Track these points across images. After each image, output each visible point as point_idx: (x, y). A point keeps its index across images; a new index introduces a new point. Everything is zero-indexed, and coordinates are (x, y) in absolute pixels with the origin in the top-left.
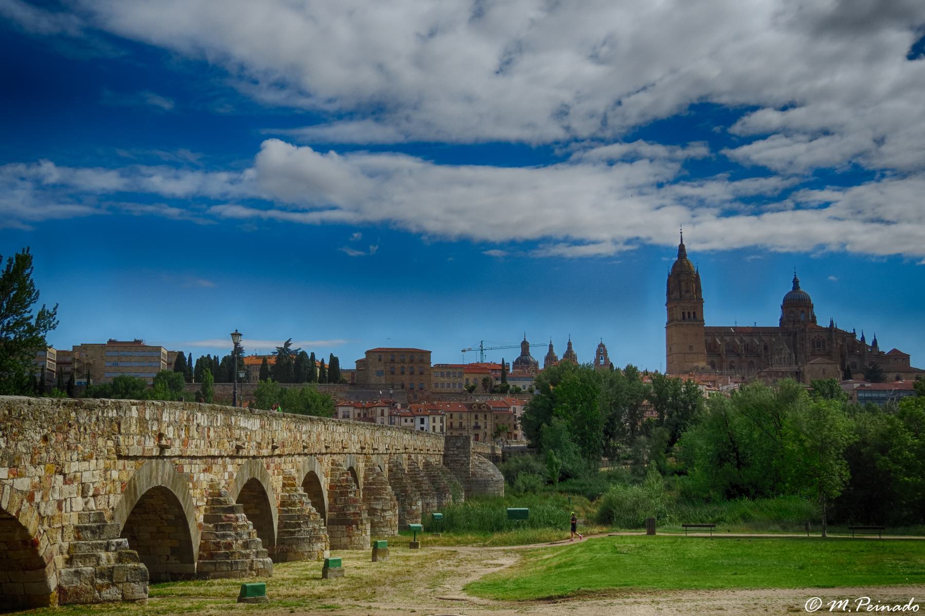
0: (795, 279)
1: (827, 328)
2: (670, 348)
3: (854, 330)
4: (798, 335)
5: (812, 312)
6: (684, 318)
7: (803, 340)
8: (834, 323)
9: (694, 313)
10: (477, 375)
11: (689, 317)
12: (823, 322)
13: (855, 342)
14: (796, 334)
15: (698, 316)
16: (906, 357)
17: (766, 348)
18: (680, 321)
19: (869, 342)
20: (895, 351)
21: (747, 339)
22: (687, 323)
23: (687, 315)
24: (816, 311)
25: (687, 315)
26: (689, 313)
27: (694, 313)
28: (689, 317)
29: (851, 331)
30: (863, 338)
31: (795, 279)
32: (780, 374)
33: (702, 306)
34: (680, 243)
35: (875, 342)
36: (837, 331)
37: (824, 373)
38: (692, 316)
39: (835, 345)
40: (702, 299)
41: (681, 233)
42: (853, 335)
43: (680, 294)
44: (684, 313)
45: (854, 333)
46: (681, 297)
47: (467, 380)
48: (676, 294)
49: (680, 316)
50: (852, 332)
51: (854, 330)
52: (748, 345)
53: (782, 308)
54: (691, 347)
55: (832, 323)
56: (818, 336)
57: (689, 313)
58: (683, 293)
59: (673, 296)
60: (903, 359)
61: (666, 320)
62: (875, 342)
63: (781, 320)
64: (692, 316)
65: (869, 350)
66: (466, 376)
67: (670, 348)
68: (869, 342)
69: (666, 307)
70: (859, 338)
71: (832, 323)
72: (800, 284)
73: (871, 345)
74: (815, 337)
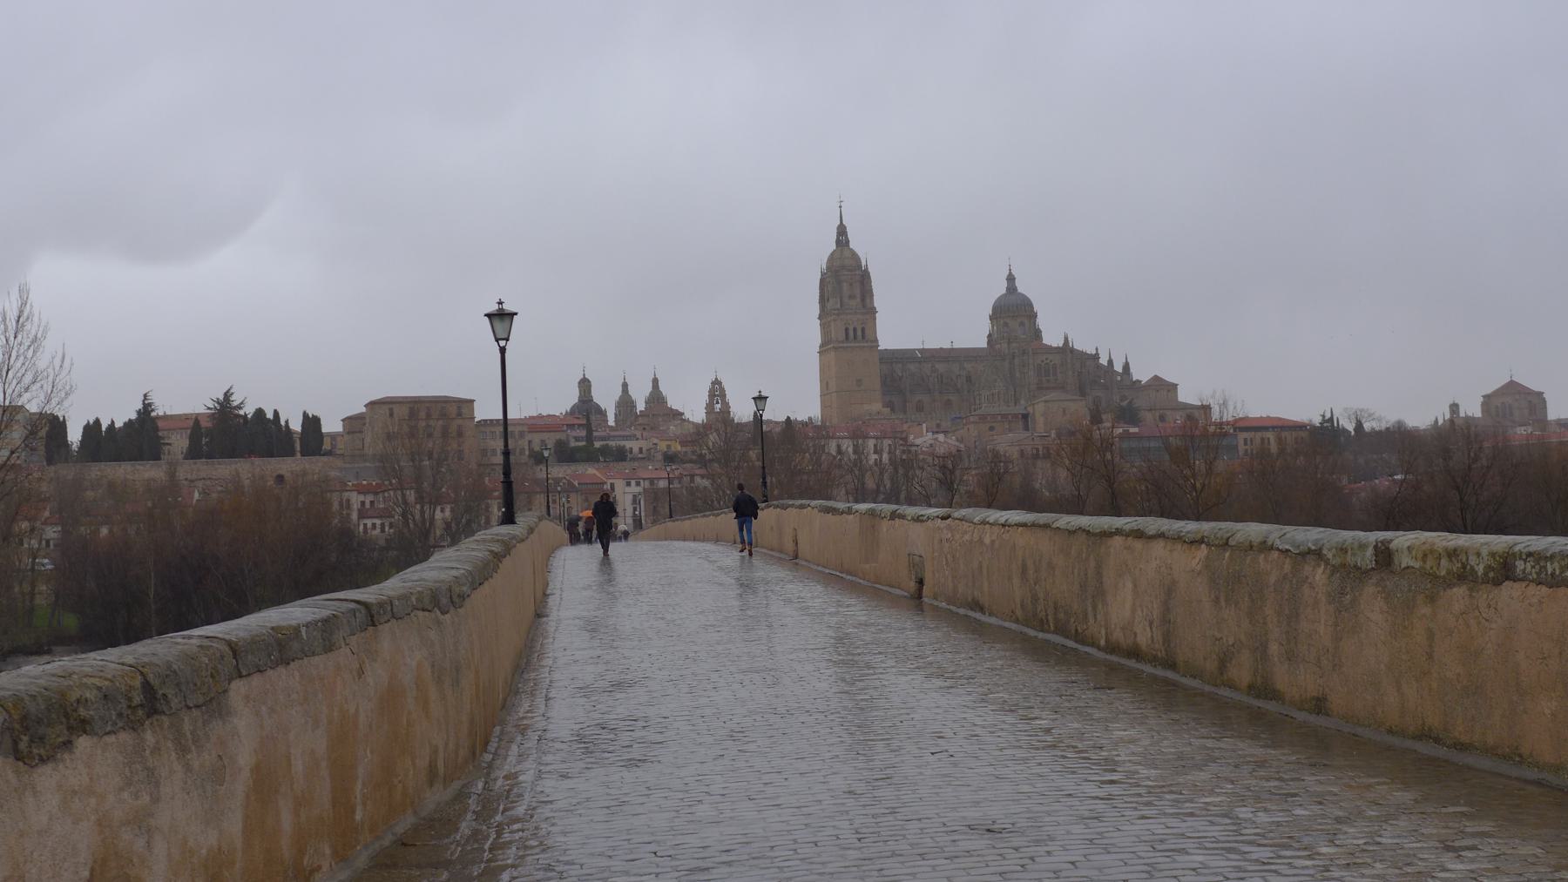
0: (1010, 274)
1: (1058, 348)
2: (827, 383)
3: (1097, 349)
4: (1016, 361)
5: (1035, 324)
7: (1024, 366)
8: (1069, 339)
10: (545, 434)
11: (855, 338)
12: (1052, 338)
13: (1099, 366)
14: (1014, 357)
15: (867, 332)
16: (1173, 387)
17: (969, 379)
18: (843, 342)
19: (1118, 368)
20: (1156, 378)
21: (941, 367)
22: (852, 345)
24: (1042, 322)
26: (855, 330)
28: (855, 338)
29: (1091, 351)
30: (1110, 362)
31: (1010, 274)
32: (999, 418)
33: (875, 319)
34: (839, 223)
35: (1126, 367)
36: (1072, 350)
38: (859, 333)
39: (1070, 373)
40: (875, 308)
41: (840, 207)
42: (1096, 357)
43: (841, 301)
44: (847, 330)
45: (1097, 354)
46: (841, 306)
47: (530, 442)
48: (833, 304)
49: (842, 336)
50: (1094, 352)
51: (1097, 349)
52: (942, 377)
53: (991, 319)
54: (859, 382)
55: (1066, 339)
56: (1047, 359)
57: (855, 330)
59: (829, 305)
60: (1169, 391)
61: (819, 341)
62: (1126, 367)
63: (990, 336)
64: (859, 333)
65: (1119, 378)
66: (529, 437)
67: (827, 383)
68: (1118, 368)
70: (1104, 361)
71: (1066, 339)
72: (1018, 283)
73: (1120, 371)
74: (1043, 361)
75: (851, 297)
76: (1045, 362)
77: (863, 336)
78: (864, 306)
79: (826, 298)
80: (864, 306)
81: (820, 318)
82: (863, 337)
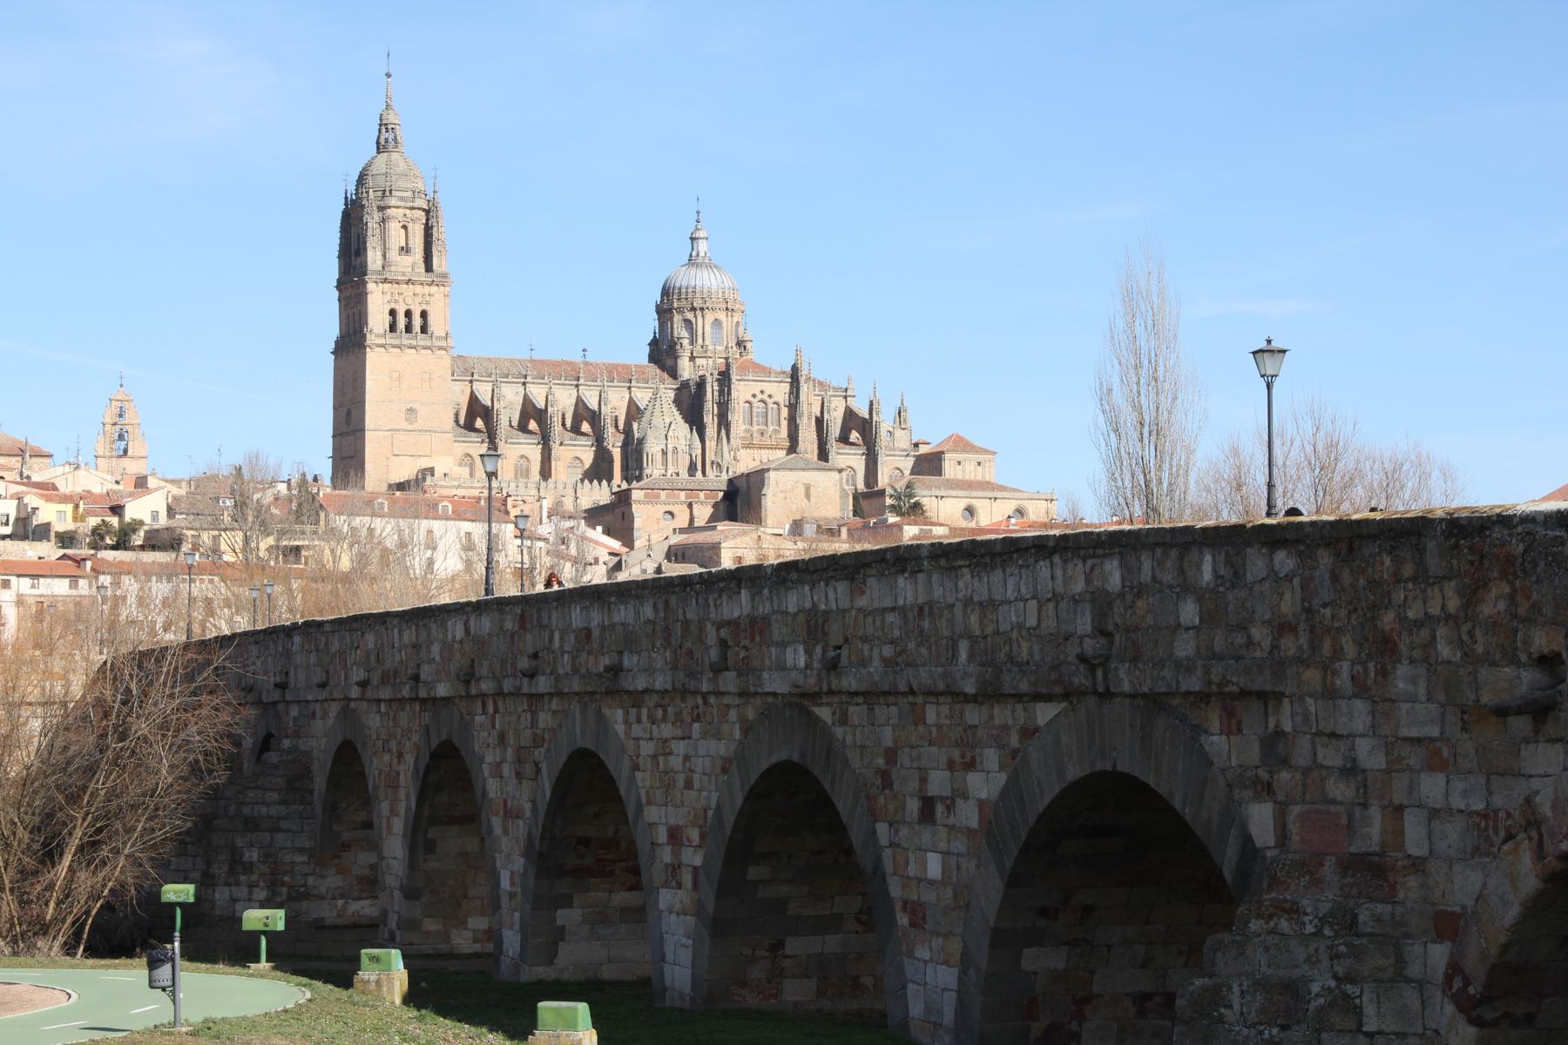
2: (349, 413)
6: (393, 328)
9: (424, 314)
11: (408, 329)
15: (431, 319)
23: (401, 322)
25: (401, 322)
26: (408, 314)
27: (424, 314)
28: (408, 329)
37: (808, 496)
38: (417, 322)
43: (384, 256)
44: (393, 313)
56: (762, 392)
57: (408, 314)
58: (393, 254)
64: (417, 322)
67: (349, 413)
69: (337, 293)
74: (754, 396)
75: (405, 250)
76: (760, 396)
77: (424, 329)
78: (429, 267)
79: (353, 248)
80: (429, 267)
81: (338, 287)
82: (424, 329)
